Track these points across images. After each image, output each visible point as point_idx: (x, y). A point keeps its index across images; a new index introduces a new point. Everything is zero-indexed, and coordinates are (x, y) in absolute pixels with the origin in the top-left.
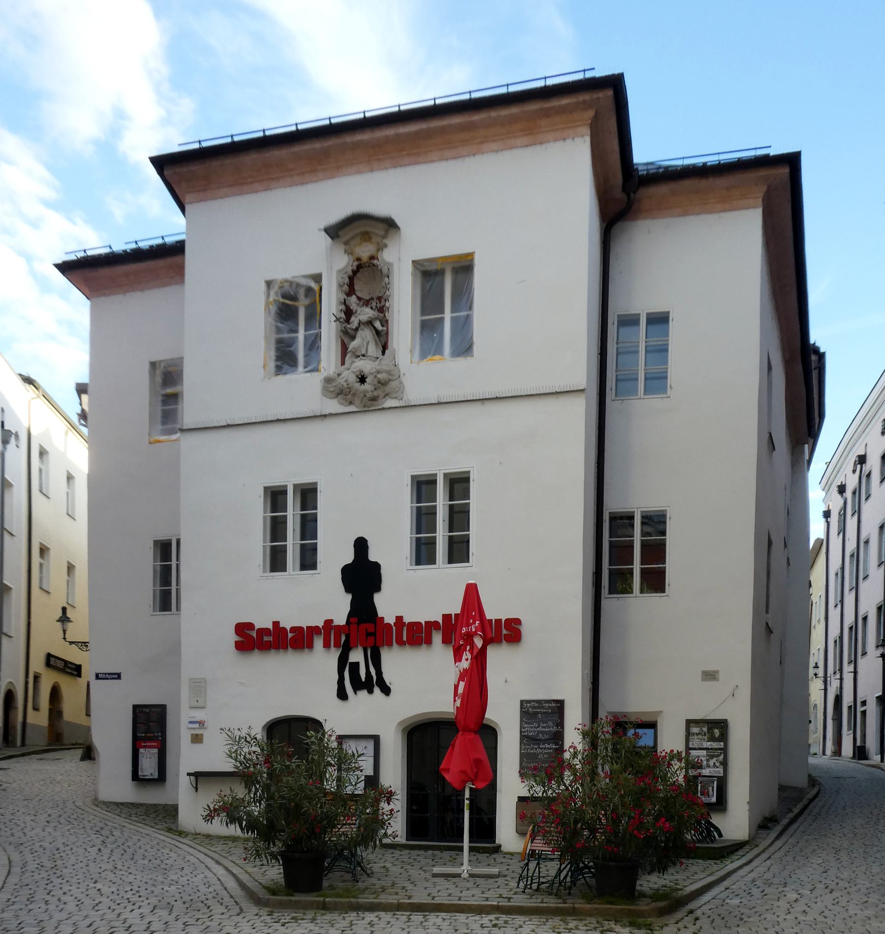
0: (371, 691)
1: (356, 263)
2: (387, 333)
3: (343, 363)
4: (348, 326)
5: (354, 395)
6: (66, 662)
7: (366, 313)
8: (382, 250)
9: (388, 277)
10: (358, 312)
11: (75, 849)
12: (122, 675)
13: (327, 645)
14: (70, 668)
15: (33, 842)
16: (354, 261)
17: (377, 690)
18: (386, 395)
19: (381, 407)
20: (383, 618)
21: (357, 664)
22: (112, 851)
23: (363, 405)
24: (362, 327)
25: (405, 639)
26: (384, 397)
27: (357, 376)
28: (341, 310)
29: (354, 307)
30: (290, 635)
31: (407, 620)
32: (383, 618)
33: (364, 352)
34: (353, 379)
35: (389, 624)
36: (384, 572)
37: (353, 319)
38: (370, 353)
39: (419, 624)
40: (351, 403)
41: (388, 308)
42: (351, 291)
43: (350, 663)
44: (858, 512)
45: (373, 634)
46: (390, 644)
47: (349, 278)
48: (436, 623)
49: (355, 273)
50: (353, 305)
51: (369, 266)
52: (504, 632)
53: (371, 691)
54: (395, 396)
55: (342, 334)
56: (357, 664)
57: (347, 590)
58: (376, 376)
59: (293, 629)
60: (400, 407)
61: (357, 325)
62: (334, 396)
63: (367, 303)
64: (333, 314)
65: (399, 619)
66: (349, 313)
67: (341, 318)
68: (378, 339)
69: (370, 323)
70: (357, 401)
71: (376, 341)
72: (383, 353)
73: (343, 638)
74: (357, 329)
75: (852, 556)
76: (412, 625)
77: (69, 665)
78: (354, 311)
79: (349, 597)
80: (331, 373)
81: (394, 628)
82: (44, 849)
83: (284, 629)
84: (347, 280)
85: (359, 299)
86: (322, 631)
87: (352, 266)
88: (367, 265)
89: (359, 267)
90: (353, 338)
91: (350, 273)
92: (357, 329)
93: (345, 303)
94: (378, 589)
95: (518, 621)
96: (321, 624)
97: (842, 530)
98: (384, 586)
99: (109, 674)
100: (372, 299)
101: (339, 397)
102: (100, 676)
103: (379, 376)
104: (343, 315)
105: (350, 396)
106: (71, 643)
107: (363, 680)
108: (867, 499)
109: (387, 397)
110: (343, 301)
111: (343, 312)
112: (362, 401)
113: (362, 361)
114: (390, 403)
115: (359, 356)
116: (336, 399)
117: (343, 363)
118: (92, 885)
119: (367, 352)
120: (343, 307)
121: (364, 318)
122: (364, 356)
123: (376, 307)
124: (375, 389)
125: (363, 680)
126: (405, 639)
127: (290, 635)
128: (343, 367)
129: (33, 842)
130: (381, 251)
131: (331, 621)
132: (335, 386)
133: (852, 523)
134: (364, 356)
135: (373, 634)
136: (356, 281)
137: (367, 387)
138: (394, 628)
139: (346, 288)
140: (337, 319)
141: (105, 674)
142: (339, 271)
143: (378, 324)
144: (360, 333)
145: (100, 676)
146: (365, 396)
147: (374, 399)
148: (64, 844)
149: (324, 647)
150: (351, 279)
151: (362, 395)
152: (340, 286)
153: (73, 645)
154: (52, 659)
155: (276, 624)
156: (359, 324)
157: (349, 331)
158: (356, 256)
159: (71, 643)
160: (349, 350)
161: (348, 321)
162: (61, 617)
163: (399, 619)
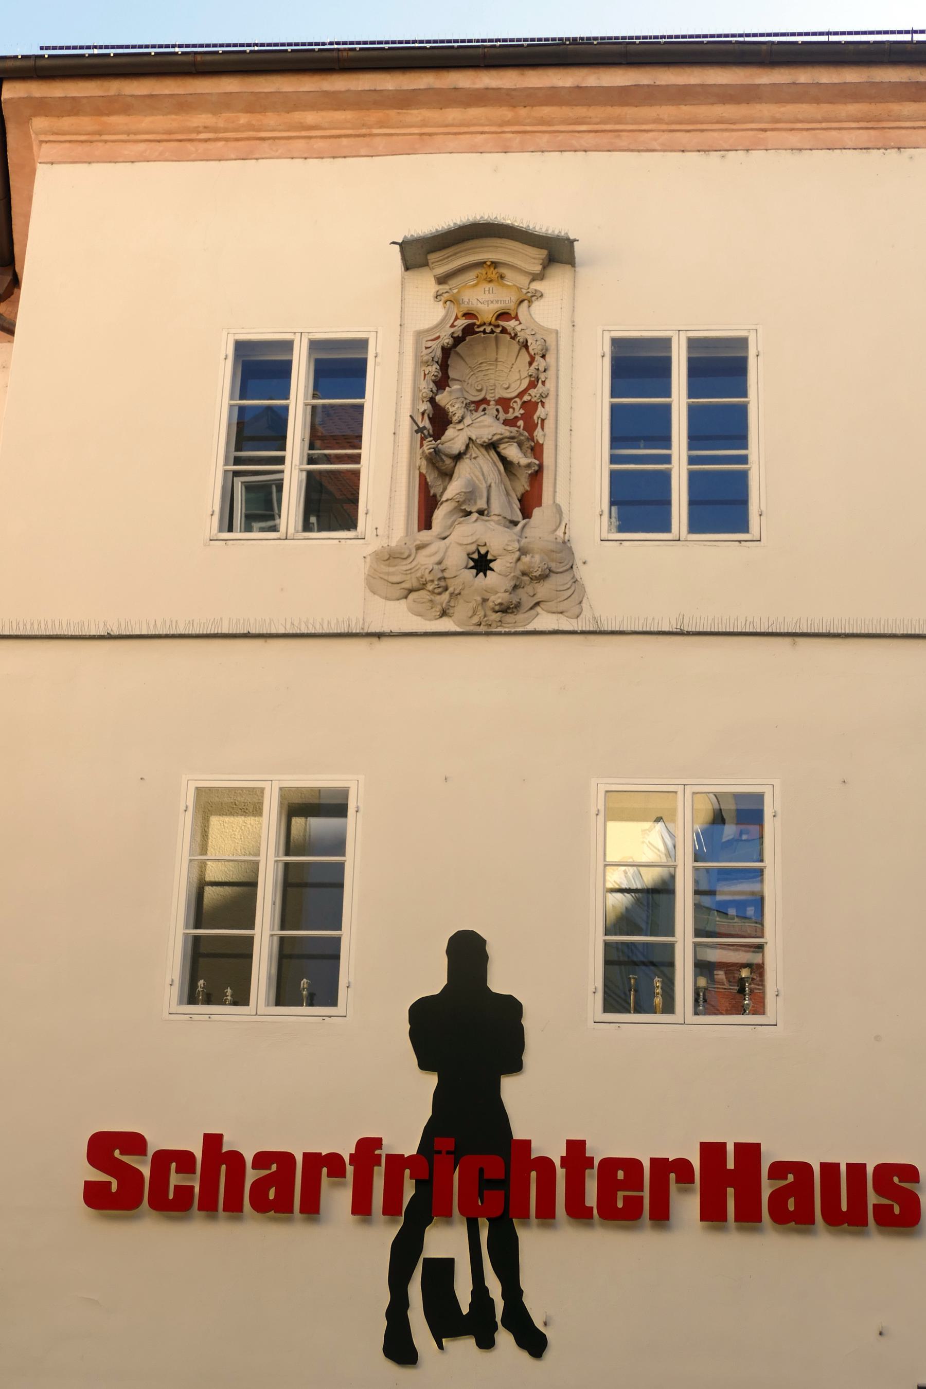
0: (486, 1342)
1: (462, 323)
2: (537, 475)
3: (426, 523)
5: (455, 595)
8: (530, 302)
13: (361, 1207)
16: (456, 318)
17: (504, 1338)
18: (538, 604)
20: (528, 1143)
21: (448, 1264)
25: (591, 1198)
26: (531, 608)
28: (423, 414)
29: (455, 409)
30: (251, 1176)
31: (598, 1150)
32: (528, 1143)
33: (481, 504)
35: (545, 1164)
36: (527, 1022)
37: (450, 432)
39: (633, 1165)
40: (444, 613)
41: (543, 420)
43: (425, 1259)
45: (501, 1184)
46: (546, 1213)
47: (444, 349)
48: (682, 1167)
49: (457, 341)
51: (492, 332)
52: (873, 1198)
53: (486, 1342)
54: (561, 607)
55: (424, 463)
56: (448, 1264)
57: (424, 1065)
59: (262, 1159)
62: (397, 591)
65: (576, 1148)
67: (424, 428)
69: (492, 446)
70: (462, 610)
72: (526, 513)
73: (409, 1191)
74: (458, 457)
76: (609, 1165)
78: (455, 419)
79: (432, 1081)
81: (561, 1173)
83: (236, 1158)
84: (439, 353)
86: (350, 1169)
87: (452, 326)
88: (488, 329)
89: (469, 330)
90: (448, 475)
91: (447, 341)
92: (458, 457)
93: (432, 401)
94: (515, 1066)
95: (910, 1173)
96: (346, 1150)
98: (529, 1057)
101: (411, 596)
104: (426, 423)
105: (446, 596)
107: (465, 1310)
109: (538, 609)
111: (426, 416)
112: (474, 613)
114: (545, 621)
115: (469, 513)
117: (426, 523)
125: (465, 1310)
126: (591, 1198)
127: (251, 1176)
130: (526, 303)
131: (377, 1142)
132: (409, 571)
134: (481, 512)
135: (501, 1184)
138: (561, 1173)
139: (434, 369)
142: (419, 334)
143: (512, 452)
147: (506, 609)
149: (354, 1211)
150: (447, 352)
151: (479, 599)
152: (421, 363)
155: (212, 1141)
156: (467, 446)
158: (464, 308)
163: (576, 1148)
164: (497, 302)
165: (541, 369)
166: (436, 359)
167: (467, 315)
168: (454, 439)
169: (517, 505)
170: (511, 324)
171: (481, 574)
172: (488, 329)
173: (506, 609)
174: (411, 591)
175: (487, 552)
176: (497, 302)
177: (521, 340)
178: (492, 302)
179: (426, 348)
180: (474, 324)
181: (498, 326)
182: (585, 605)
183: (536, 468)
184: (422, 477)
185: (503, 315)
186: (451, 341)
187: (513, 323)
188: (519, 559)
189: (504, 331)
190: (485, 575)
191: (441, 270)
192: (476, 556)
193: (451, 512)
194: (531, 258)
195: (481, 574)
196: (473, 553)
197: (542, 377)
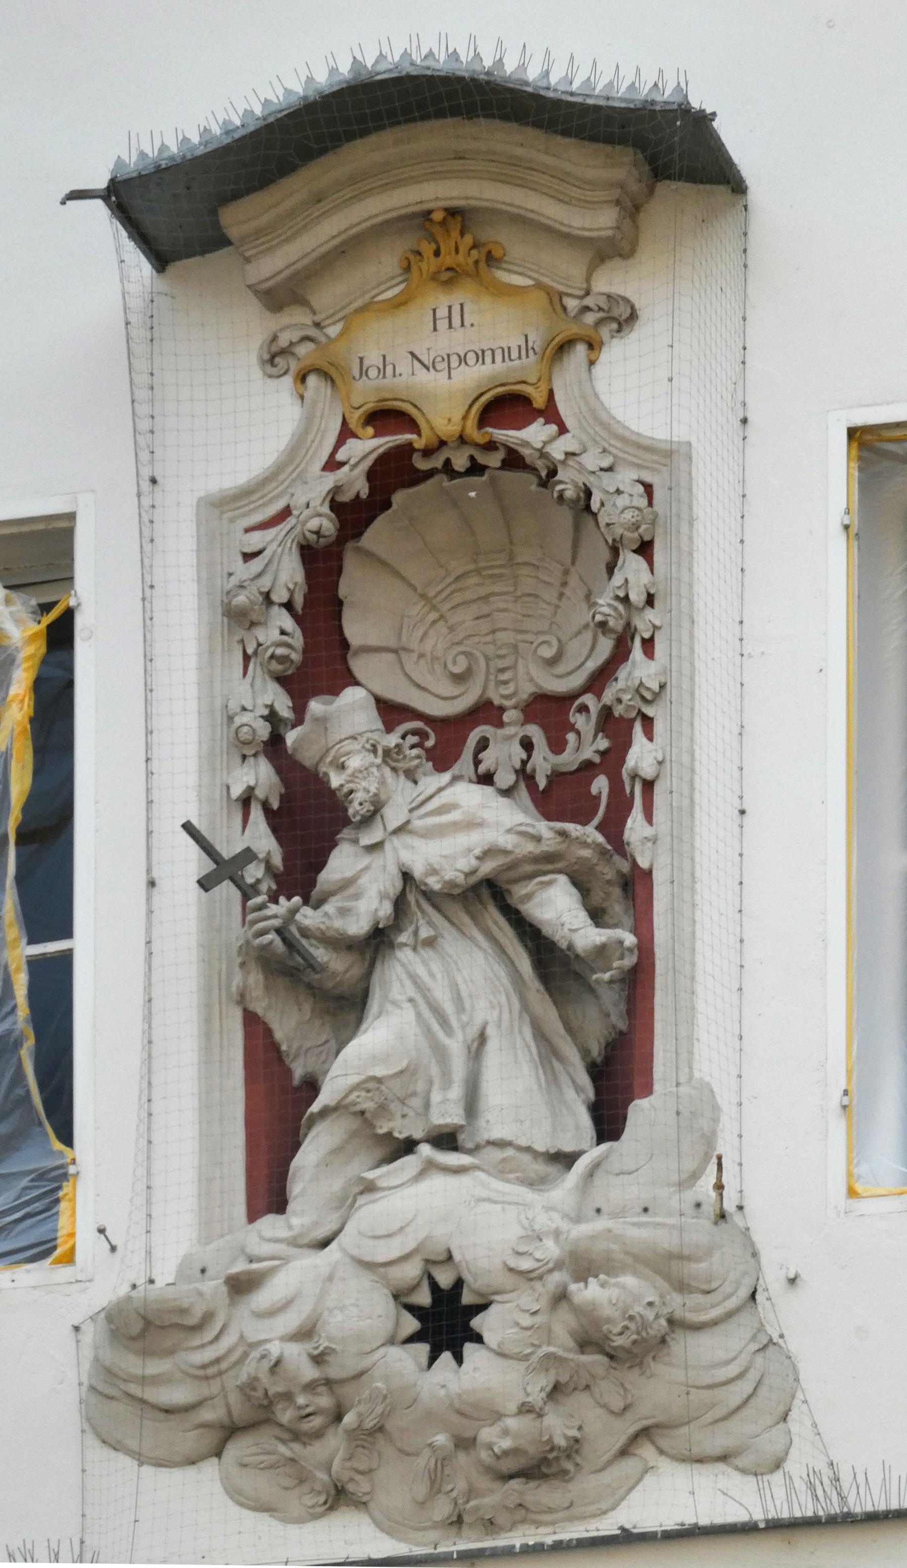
4: (308, 917)
8: (594, 345)
9: (645, 549)
10: (394, 816)
16: (346, 433)
18: (644, 1433)
19: (607, 1526)
23: (442, 1509)
26: (624, 1453)
27: (396, 1297)
28: (246, 801)
50: (354, 763)
51: (476, 469)
58: (561, 1297)
60: (776, 1526)
61: (387, 909)
64: (188, 827)
67: (248, 855)
71: (540, 1035)
78: (355, 809)
80: (165, 1274)
87: (332, 465)
88: (460, 462)
109: (647, 1451)
110: (264, 731)
111: (257, 813)
128: (270, 1224)
130: (581, 349)
146: (465, 1443)
156: (400, 904)
164: (480, 356)
165: (636, 597)
166: (280, 596)
169: (579, 1089)
171: (446, 1357)
172: (460, 462)
175: (459, 1284)
176: (480, 356)
177: (570, 494)
178: (463, 360)
179: (248, 557)
180: (407, 450)
181: (491, 446)
183: (629, 961)
186: (328, 525)
190: (459, 1360)
192: (424, 1298)
195: (446, 1357)
196: (414, 1288)
197: (644, 622)
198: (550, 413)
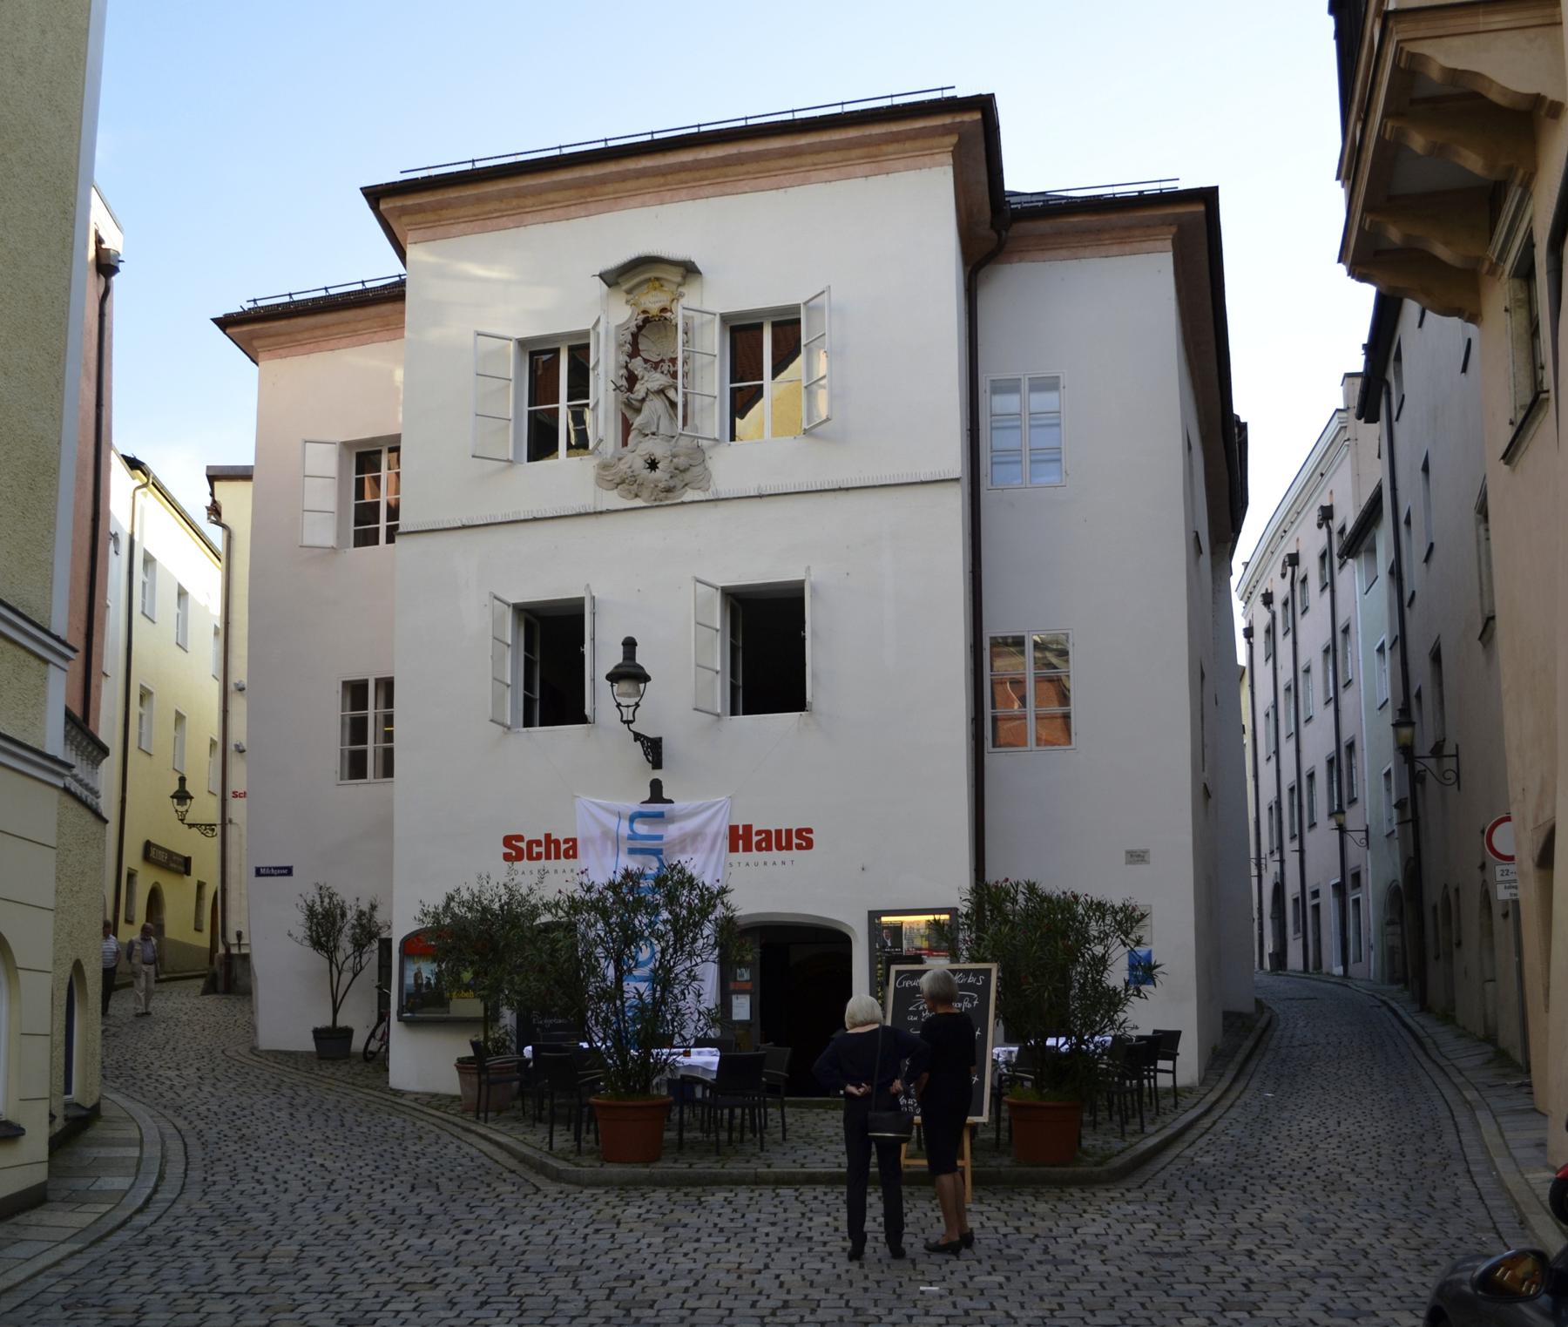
1: (642, 316)
3: (625, 444)
4: (632, 396)
5: (641, 485)
6: (170, 854)
7: (655, 380)
10: (646, 378)
11: (258, 1114)
12: (294, 870)
14: (175, 862)
15: (194, 1104)
22: (309, 1116)
24: (651, 396)
29: (639, 372)
34: (639, 464)
37: (638, 386)
38: (662, 431)
42: (635, 352)
44: (1293, 630)
47: (632, 334)
49: (640, 328)
55: (623, 407)
63: (656, 366)
66: (632, 379)
68: (672, 412)
69: (661, 392)
70: (645, 493)
71: (670, 415)
74: (643, 400)
75: (1288, 689)
77: (175, 858)
80: (609, 457)
82: (216, 1114)
84: (629, 338)
85: (646, 361)
89: (646, 321)
90: (638, 411)
92: (643, 400)
93: (626, 367)
97: (1272, 654)
99: (275, 868)
100: (662, 361)
102: (262, 871)
103: (675, 460)
104: (624, 383)
106: (191, 826)
108: (1303, 613)
112: (652, 494)
113: (651, 441)
115: (647, 435)
116: (615, 491)
117: (625, 444)
118: (308, 1160)
119: (658, 429)
120: (624, 372)
121: (654, 386)
122: (653, 434)
123: (669, 371)
124: (671, 477)
129: (194, 1104)
133: (1284, 646)
134: (653, 434)
136: (641, 339)
137: (658, 474)
139: (628, 348)
140: (617, 388)
141: (270, 868)
142: (618, 327)
144: (646, 408)
145: (262, 871)
146: (657, 486)
148: (238, 1106)
150: (635, 336)
152: (620, 346)
153: (194, 829)
154: (153, 850)
156: (647, 394)
157: (634, 402)
159: (191, 826)
160: (634, 427)
161: (631, 389)
162: (177, 792)
167: (644, 312)
168: (640, 390)
170: (668, 315)
173: (669, 490)
174: (618, 484)
182: (711, 483)
184: (623, 414)
185: (664, 310)
187: (668, 315)
188: (671, 461)
189: (666, 319)
191: (626, 286)
193: (636, 436)
194: (674, 275)
198: (671, 311)
